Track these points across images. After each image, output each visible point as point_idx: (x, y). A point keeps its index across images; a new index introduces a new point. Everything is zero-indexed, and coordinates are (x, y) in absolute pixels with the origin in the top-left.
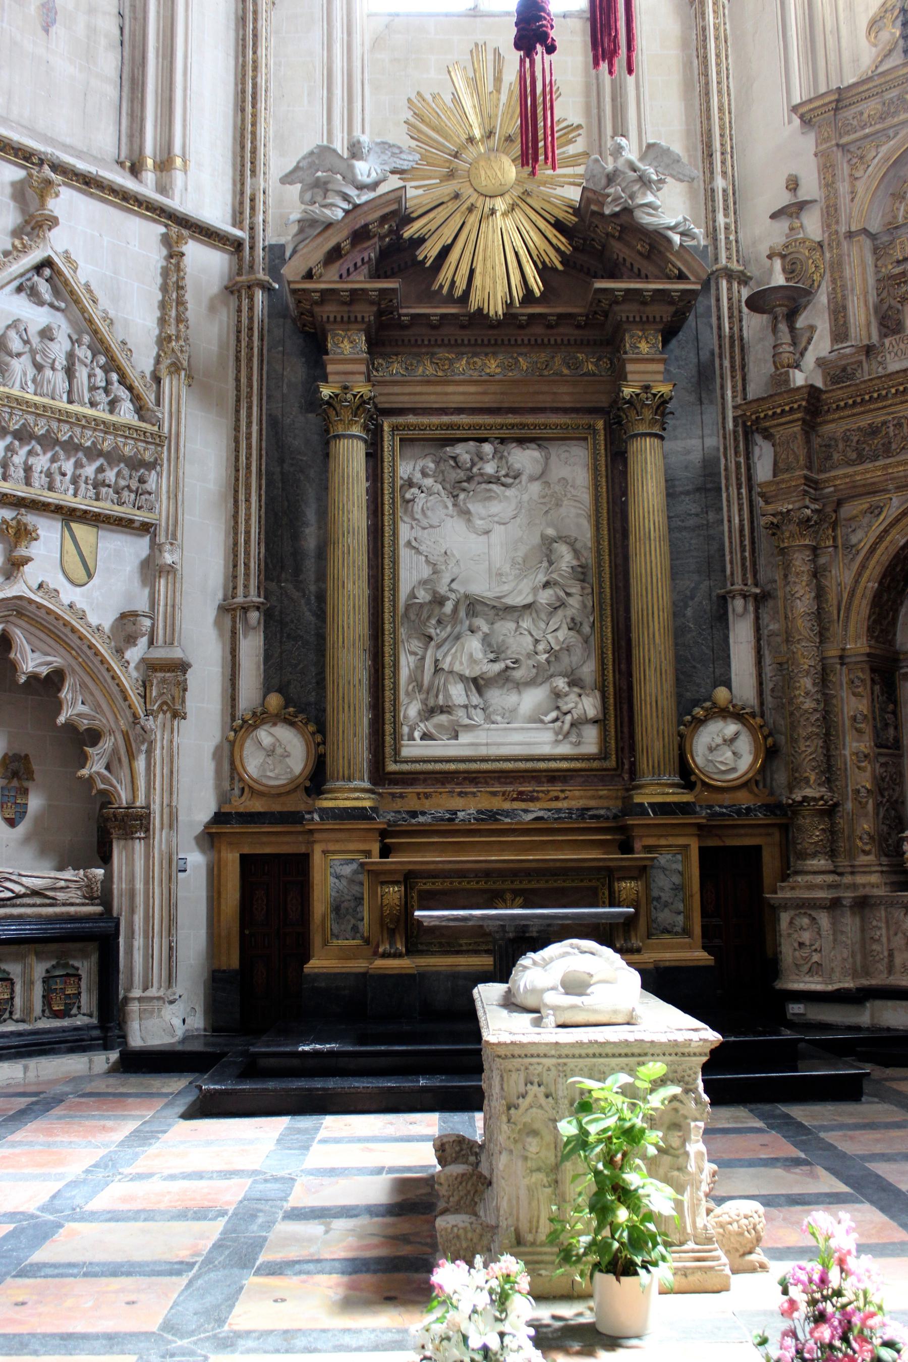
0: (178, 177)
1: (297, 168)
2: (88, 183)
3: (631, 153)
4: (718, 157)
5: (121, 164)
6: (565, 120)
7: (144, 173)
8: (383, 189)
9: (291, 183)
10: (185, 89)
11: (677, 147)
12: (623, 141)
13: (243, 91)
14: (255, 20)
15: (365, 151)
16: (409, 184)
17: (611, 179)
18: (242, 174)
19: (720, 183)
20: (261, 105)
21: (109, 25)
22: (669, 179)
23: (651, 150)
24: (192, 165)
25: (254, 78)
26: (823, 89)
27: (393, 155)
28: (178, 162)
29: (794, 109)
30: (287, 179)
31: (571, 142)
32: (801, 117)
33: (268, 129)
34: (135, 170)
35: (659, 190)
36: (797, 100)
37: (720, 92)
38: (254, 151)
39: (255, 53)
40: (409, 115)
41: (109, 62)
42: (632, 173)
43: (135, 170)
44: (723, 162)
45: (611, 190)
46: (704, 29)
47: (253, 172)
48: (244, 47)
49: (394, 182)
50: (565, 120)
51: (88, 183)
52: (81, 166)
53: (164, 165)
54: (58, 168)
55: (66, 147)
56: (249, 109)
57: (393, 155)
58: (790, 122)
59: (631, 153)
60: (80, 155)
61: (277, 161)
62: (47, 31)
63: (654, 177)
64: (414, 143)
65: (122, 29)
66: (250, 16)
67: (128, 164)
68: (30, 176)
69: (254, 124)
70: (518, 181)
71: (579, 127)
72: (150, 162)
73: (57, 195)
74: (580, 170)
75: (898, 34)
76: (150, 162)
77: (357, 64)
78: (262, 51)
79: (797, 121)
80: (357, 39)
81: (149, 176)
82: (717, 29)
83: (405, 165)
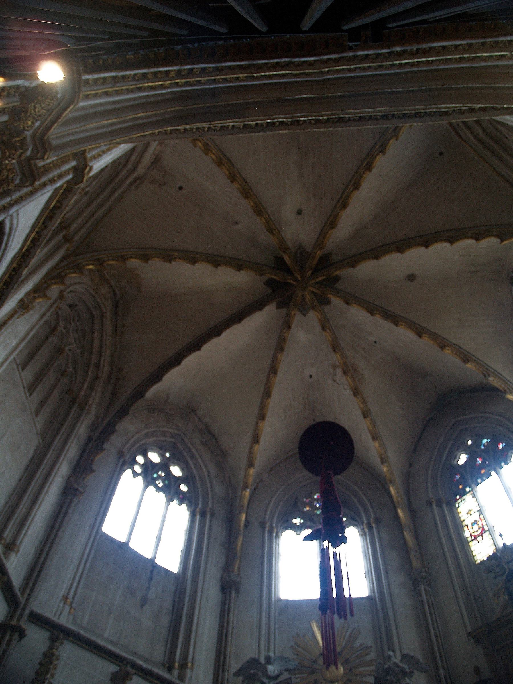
0: (189, 672)
1: (241, 669)
2: (146, 674)
3: (397, 659)
4: (438, 658)
5: (163, 665)
6: (364, 644)
7: (173, 671)
8: (281, 678)
9: (238, 676)
10: (196, 632)
11: (419, 656)
12: (391, 653)
13: (222, 633)
14: (229, 603)
15: (272, 660)
16: (293, 677)
17: (388, 671)
18: (218, 672)
19: (442, 672)
20: (229, 639)
21: (168, 604)
22: (415, 671)
23: (405, 657)
24: (196, 666)
25: (227, 628)
26: (480, 624)
27: (286, 662)
28: (189, 665)
29: (469, 634)
30: (237, 674)
31: (367, 654)
32: (474, 638)
33: (231, 651)
34: (170, 669)
35: (412, 676)
36: (469, 630)
37: (434, 628)
38: (225, 659)
39: (228, 616)
40: (293, 643)
41: (165, 620)
42: (397, 669)
43: (170, 669)
44: (442, 662)
45: (388, 678)
46: (422, 601)
47: (223, 670)
48: (224, 615)
49: (285, 676)
50: (364, 644)
51: (146, 674)
52: (145, 665)
53: (183, 666)
54: (135, 666)
55: (140, 657)
56: (224, 640)
57: (286, 662)
58: (469, 640)
59: (397, 659)
60: (145, 660)
61: (234, 666)
62: (142, 606)
63: (408, 670)
64: (295, 657)
65: (173, 607)
66: (227, 602)
67: (167, 665)
68: (120, 670)
69: (225, 648)
70: (345, 674)
71: (371, 647)
72: (177, 665)
73: (131, 679)
74: (373, 668)
75: (507, 598)
76: (177, 665)
77: (272, 621)
78: (231, 616)
79: (472, 640)
80: (273, 610)
81: (176, 672)
82: (428, 601)
83: (291, 667)
